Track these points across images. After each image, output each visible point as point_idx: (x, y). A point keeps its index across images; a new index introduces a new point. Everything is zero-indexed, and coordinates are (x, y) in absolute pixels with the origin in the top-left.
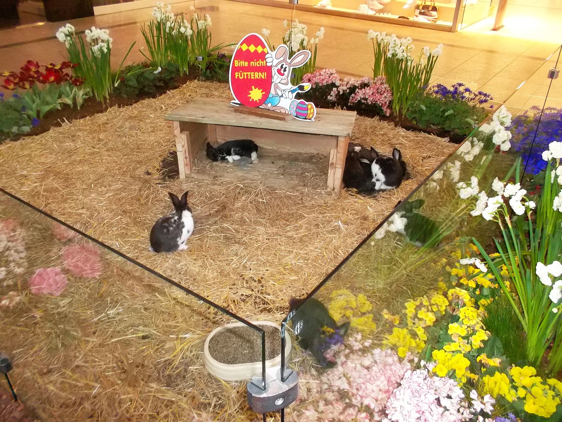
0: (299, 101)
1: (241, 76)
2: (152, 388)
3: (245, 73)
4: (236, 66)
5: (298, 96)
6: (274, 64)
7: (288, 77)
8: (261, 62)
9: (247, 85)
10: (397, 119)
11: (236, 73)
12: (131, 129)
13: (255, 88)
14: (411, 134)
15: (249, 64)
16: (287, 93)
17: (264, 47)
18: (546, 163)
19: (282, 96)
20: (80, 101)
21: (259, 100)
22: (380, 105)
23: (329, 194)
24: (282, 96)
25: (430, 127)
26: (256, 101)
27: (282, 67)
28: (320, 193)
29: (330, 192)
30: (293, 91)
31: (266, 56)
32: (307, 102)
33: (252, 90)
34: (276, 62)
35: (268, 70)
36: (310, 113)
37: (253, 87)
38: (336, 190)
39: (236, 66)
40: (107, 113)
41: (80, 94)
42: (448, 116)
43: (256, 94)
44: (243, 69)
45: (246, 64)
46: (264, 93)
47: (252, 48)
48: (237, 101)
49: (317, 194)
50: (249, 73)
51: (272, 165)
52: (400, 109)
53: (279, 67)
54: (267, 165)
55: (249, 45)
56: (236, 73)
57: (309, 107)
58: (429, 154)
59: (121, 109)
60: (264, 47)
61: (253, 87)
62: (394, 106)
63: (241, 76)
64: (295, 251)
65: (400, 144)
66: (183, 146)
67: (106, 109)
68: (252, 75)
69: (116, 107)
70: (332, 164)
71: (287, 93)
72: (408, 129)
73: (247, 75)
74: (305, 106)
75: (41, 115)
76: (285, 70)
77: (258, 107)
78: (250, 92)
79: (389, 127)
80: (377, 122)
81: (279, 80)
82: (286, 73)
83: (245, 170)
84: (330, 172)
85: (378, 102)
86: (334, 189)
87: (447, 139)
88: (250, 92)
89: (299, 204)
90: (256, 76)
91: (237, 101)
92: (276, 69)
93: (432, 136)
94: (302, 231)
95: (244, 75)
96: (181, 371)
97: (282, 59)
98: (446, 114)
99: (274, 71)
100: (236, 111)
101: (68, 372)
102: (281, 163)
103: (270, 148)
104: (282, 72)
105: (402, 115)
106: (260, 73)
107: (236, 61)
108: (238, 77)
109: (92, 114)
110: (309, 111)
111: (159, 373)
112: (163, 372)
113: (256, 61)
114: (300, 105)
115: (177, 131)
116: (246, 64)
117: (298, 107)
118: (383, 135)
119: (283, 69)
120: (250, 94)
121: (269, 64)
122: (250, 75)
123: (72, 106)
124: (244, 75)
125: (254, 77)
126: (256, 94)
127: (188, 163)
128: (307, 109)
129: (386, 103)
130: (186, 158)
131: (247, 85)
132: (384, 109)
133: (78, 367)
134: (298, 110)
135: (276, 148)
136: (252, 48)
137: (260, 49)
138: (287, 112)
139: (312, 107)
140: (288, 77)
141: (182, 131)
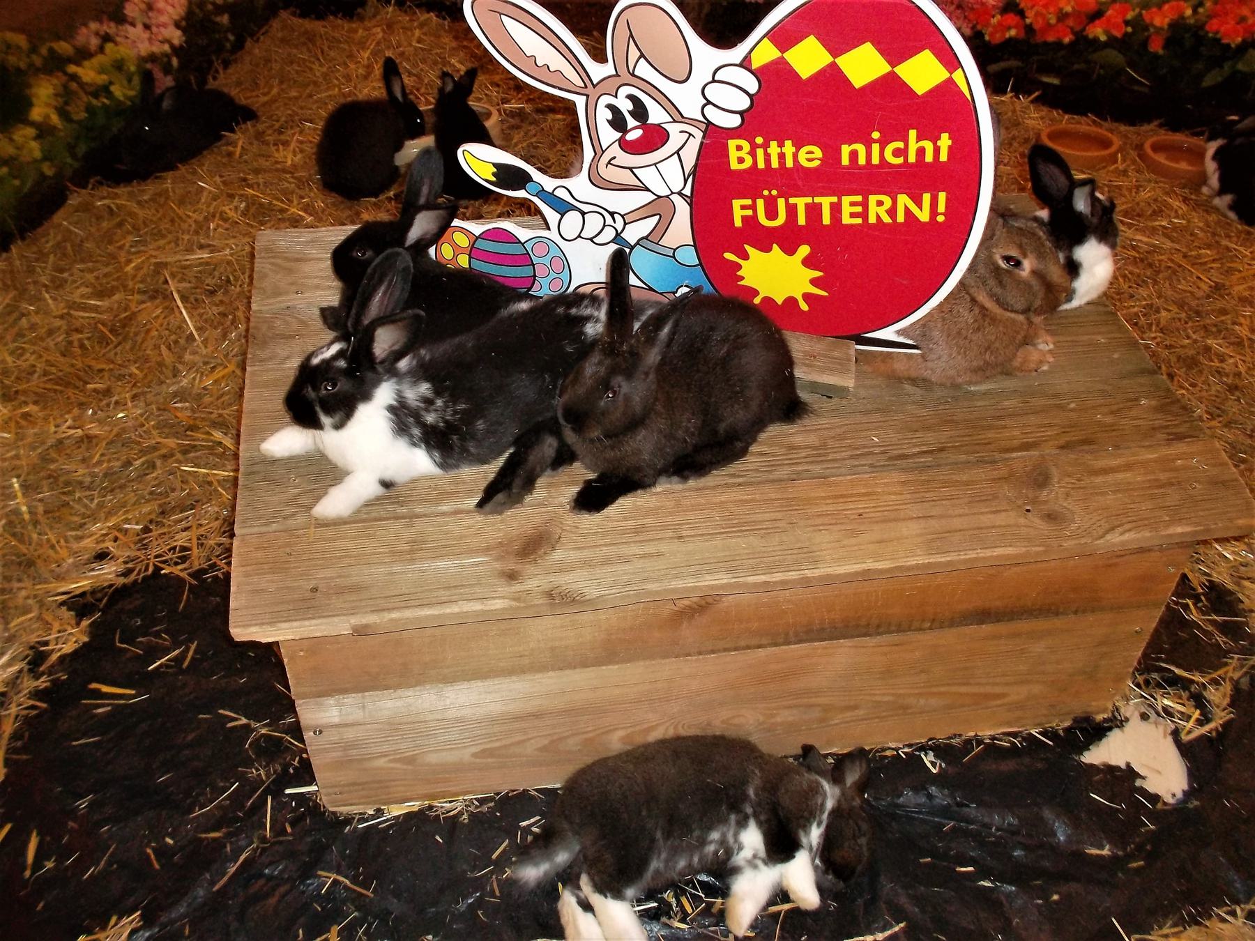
1: (772, 213)
3: (801, 203)
4: (734, 165)
8: (913, 146)
11: (737, 204)
15: (832, 155)
39: (734, 165)
45: (810, 156)
50: (826, 202)
56: (737, 204)
63: (772, 213)
68: (847, 210)
73: (814, 211)
95: (792, 210)
106: (903, 200)
108: (750, 221)
116: (810, 156)
122: (836, 209)
124: (792, 210)
125: (864, 215)
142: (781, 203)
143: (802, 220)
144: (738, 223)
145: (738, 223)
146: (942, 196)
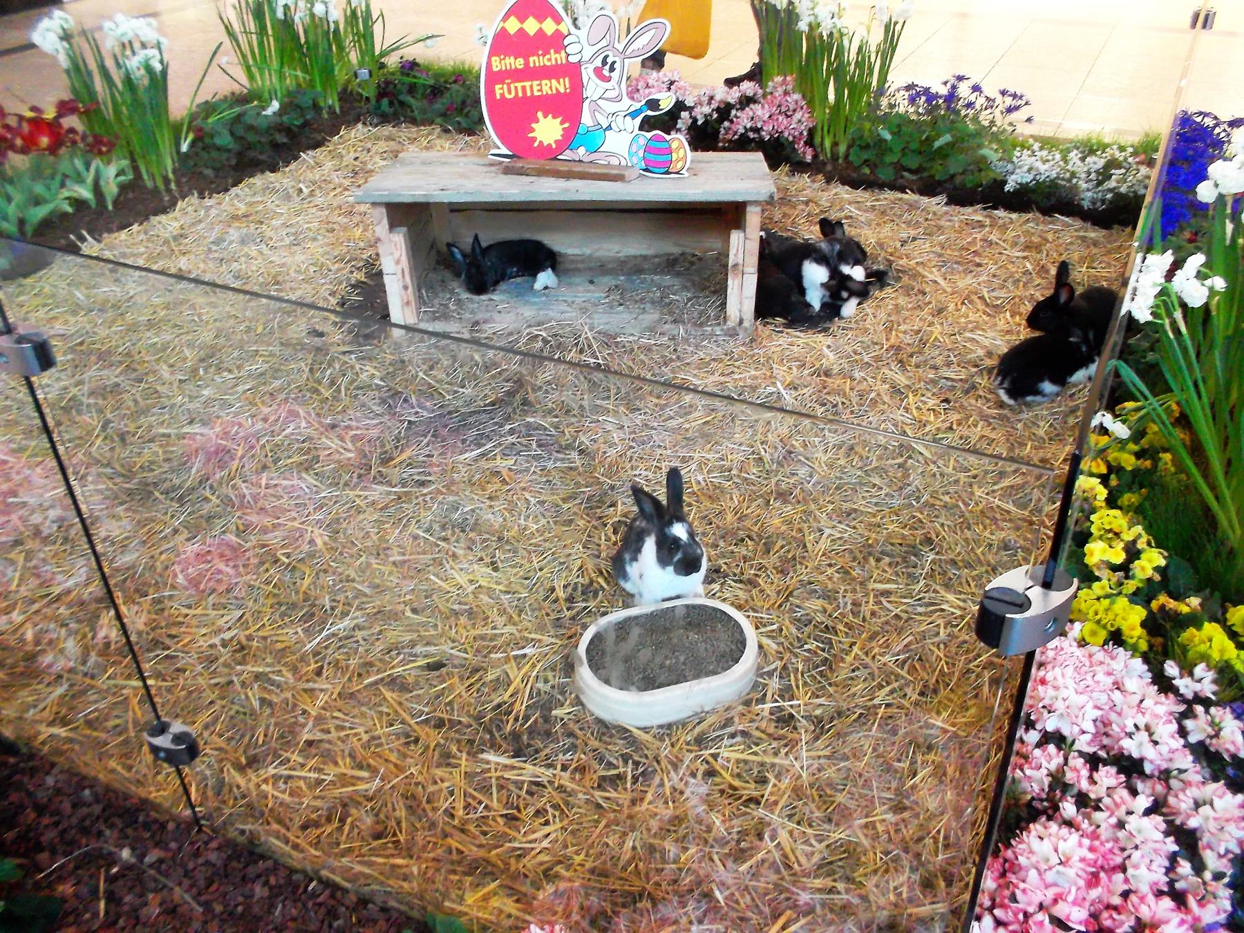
0: (649, 135)
1: (510, 92)
2: (488, 762)
3: (519, 85)
4: (495, 69)
5: (647, 125)
6: (586, 58)
7: (619, 83)
9: (529, 108)
10: (829, 168)
11: (498, 87)
12: (243, 242)
13: (545, 116)
14: (861, 195)
15: (527, 64)
16: (620, 119)
17: (558, 20)
18: (1204, 207)
19: (609, 128)
20: (111, 189)
21: (556, 142)
22: (791, 138)
23: (732, 334)
24: (609, 128)
25: (902, 177)
26: (550, 145)
27: (604, 62)
28: (713, 334)
29: (734, 328)
30: (633, 115)
31: (566, 42)
32: (669, 134)
33: (537, 121)
34: (588, 52)
35: (572, 71)
36: (678, 161)
37: (540, 114)
38: (746, 324)
39: (495, 69)
40: (177, 213)
41: (111, 174)
42: (940, 148)
43: (547, 130)
44: (517, 75)
46: (566, 125)
47: (531, 26)
48: (504, 151)
49: (704, 337)
50: (527, 84)
51: (592, 287)
52: (835, 144)
53: (598, 63)
54: (581, 289)
55: (522, 20)
56: (498, 87)
57: (674, 145)
58: (913, 233)
59: (208, 202)
60: (558, 20)
61: (540, 114)
62: (817, 140)
63: (510, 92)
64: (696, 455)
65: (846, 218)
66: (398, 262)
67: (173, 204)
68: (536, 88)
69: (194, 199)
70: (736, 265)
71: (620, 119)
72: (855, 185)
73: (524, 88)
74: (664, 145)
75: (29, 230)
76: (612, 69)
77: (555, 159)
78: (533, 125)
79: (816, 185)
80: (786, 179)
81: (599, 92)
82: (615, 75)
83: (535, 304)
84: (733, 284)
85: (786, 134)
86: (741, 322)
87: (942, 199)
88: (533, 125)
89: (671, 360)
90: (546, 90)
91: (504, 151)
92: (591, 67)
93: (910, 196)
94: (696, 414)
96: (536, 720)
97: (604, 43)
98: (937, 144)
99: (587, 73)
100: (508, 171)
101: (296, 758)
102: (609, 281)
103: (577, 251)
104: (606, 72)
105: (838, 158)
106: (554, 82)
107: (494, 59)
108: (502, 95)
109: (144, 217)
110: (674, 156)
111: (490, 732)
112: (499, 729)
113: (544, 55)
114: (652, 144)
115: (382, 228)
116: (519, 64)
117: (648, 149)
118: (807, 203)
119: (607, 67)
120: (532, 130)
121: (573, 59)
122: (531, 87)
123: (93, 204)
125: (541, 90)
126: (547, 130)
127: (412, 298)
128: (669, 151)
129: (801, 133)
130: (406, 288)
131: (529, 108)
132: (800, 147)
133: (310, 743)
134: (651, 157)
135: (588, 251)
136: (531, 26)
137: (549, 27)
138: (624, 163)
139: (681, 146)
140: (619, 83)
141: (393, 226)
142: (512, 86)
143: (520, 94)
144: (498, 97)
145: (498, 97)
146: (567, 80)
